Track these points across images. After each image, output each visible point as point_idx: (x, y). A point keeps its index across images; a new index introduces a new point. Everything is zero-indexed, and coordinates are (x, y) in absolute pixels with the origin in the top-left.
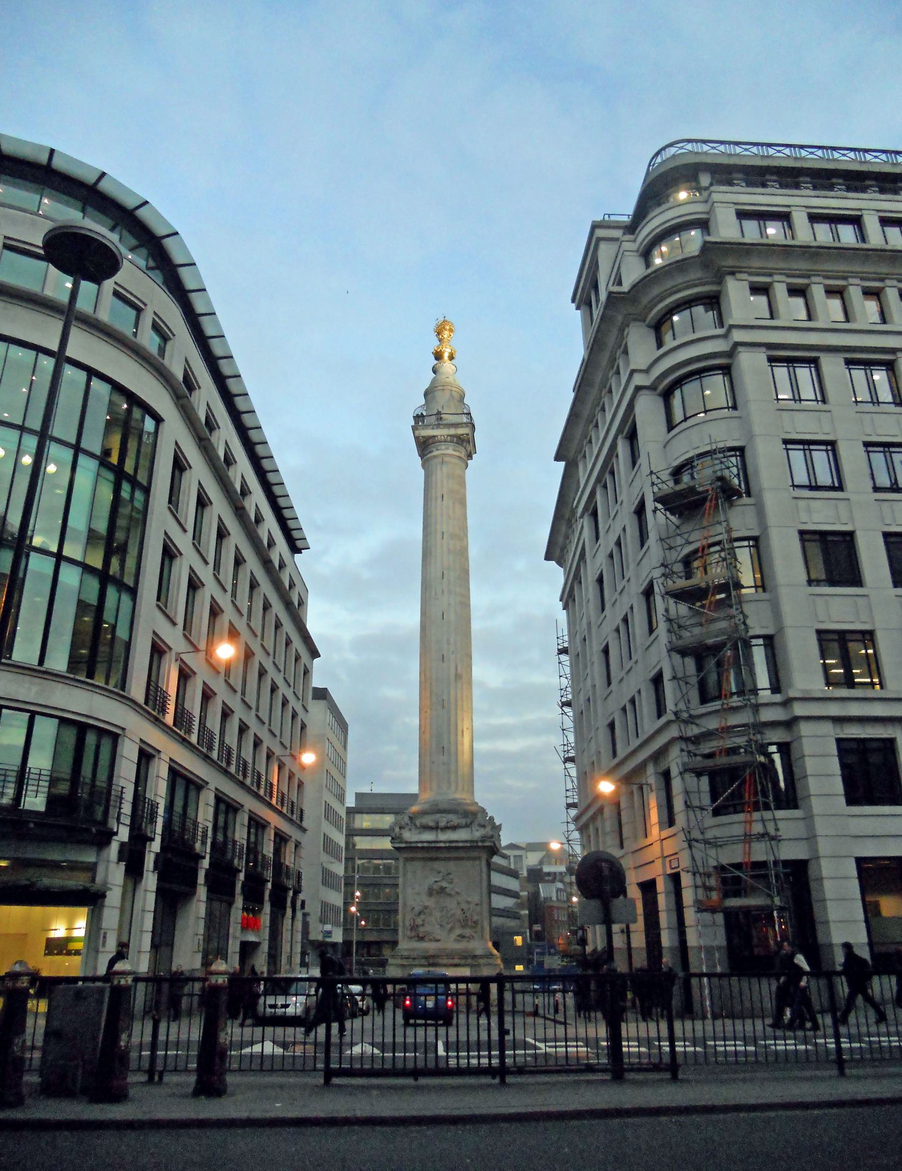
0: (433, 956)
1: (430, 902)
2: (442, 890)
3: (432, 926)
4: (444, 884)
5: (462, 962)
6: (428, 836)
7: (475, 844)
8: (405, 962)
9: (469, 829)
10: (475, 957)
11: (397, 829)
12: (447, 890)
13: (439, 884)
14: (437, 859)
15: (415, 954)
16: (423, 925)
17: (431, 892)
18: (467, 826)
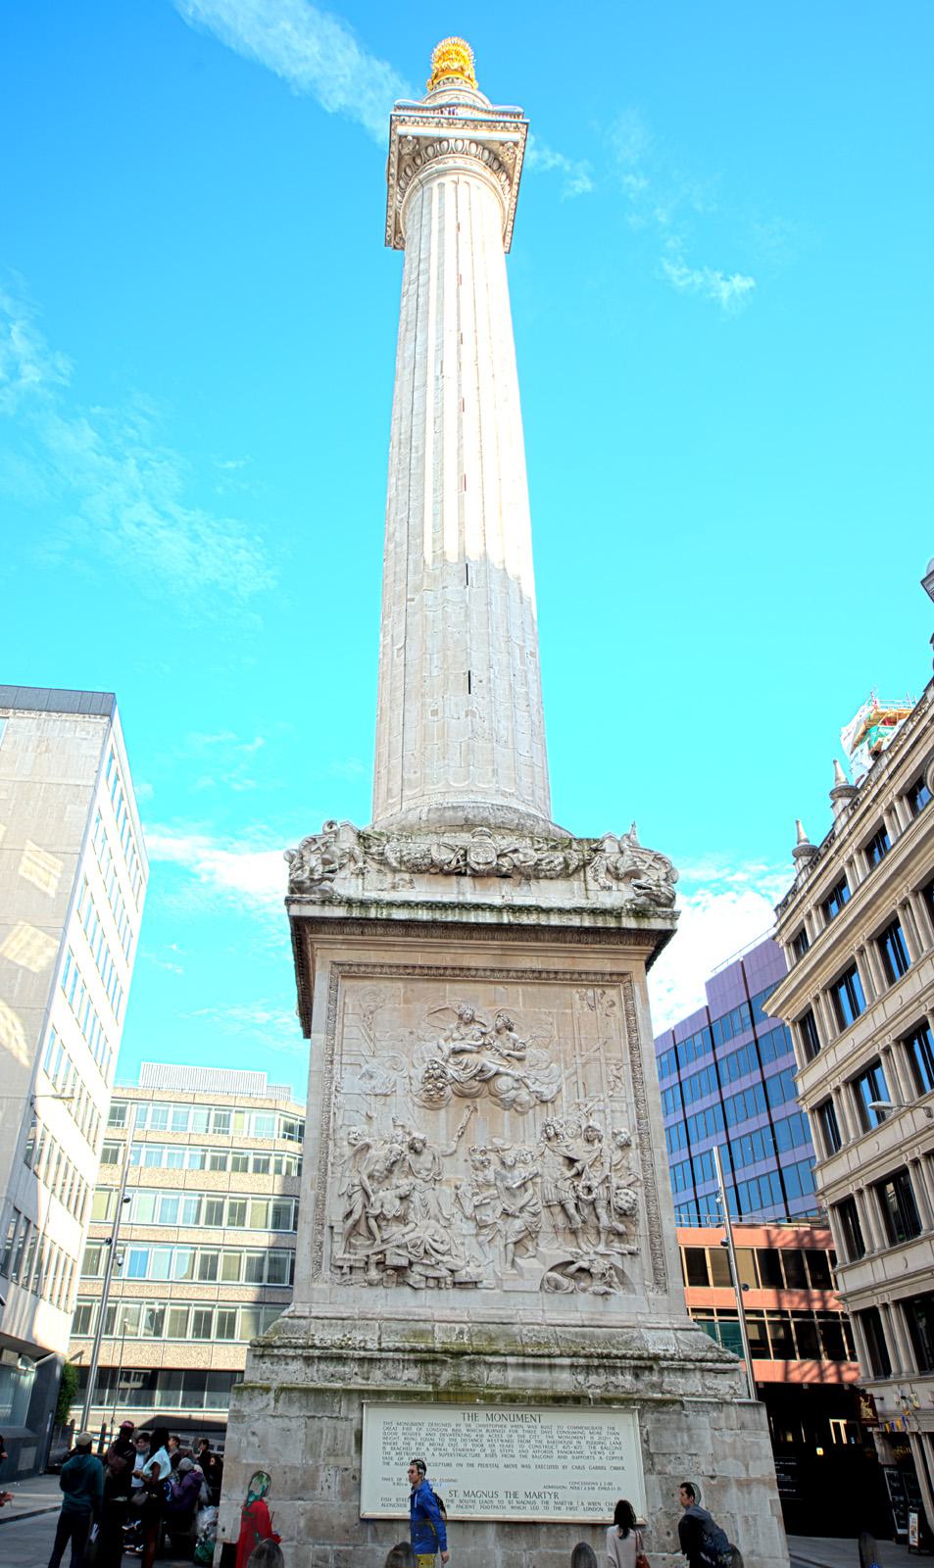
0: (458, 1354)
1: (437, 1130)
2: (484, 1077)
3: (439, 1222)
4: (490, 1062)
5: (595, 1383)
6: (425, 890)
7: (612, 923)
8: (316, 1376)
9: (576, 884)
10: (646, 1364)
11: (314, 861)
12: (503, 1083)
13: (465, 1058)
14: (461, 974)
15: (368, 1339)
16: (402, 1219)
17: (435, 1092)
18: (566, 873)
